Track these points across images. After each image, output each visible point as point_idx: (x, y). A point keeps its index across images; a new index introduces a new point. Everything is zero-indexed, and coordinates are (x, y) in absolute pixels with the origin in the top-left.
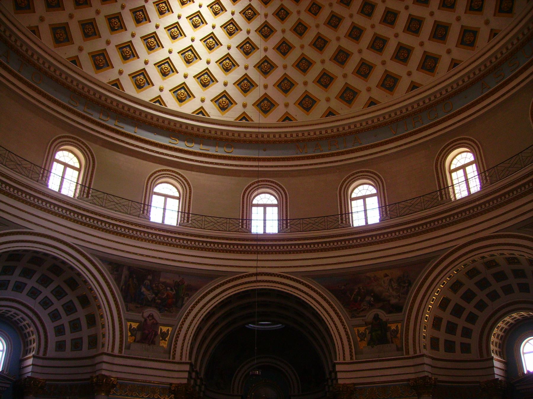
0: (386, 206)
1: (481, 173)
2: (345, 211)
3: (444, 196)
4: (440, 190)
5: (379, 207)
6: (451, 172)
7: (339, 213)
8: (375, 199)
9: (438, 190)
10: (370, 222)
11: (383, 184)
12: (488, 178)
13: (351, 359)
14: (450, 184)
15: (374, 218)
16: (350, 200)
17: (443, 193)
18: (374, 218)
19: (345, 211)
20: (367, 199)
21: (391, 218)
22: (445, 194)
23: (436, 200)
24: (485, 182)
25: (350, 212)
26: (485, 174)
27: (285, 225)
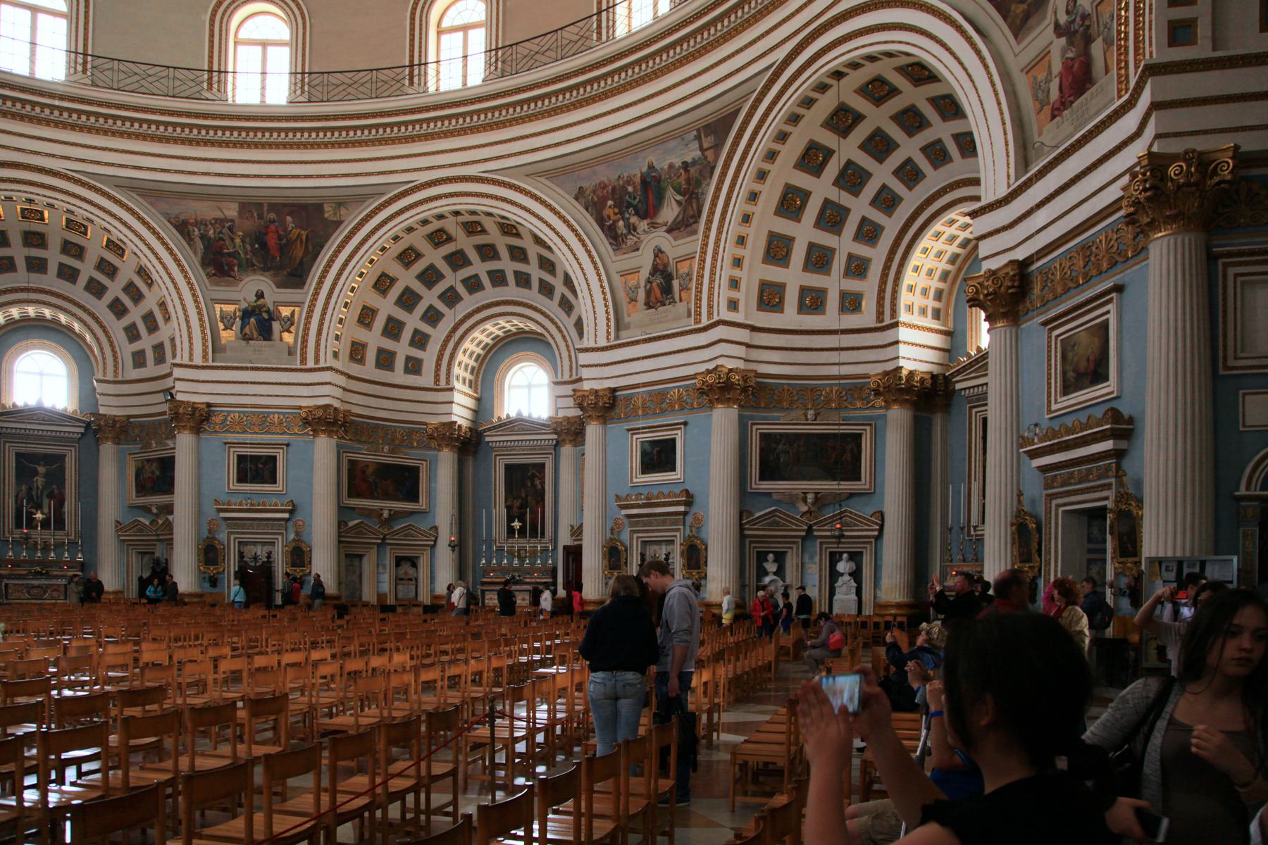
0: (303, 73)
1: (491, 51)
2: (220, 65)
3: (416, 80)
4: (412, 66)
5: (291, 73)
6: (440, 33)
7: (206, 68)
8: (286, 52)
9: (407, 64)
10: (270, 100)
11: (304, 24)
12: (499, 63)
13: (205, 357)
14: (432, 57)
15: (279, 93)
16: (235, 42)
17: (416, 72)
18: (279, 93)
19: (220, 65)
20: (270, 49)
21: (309, 102)
22: (419, 75)
23: (399, 85)
24: (493, 68)
25: (230, 69)
26: (496, 54)
27: (80, 68)
